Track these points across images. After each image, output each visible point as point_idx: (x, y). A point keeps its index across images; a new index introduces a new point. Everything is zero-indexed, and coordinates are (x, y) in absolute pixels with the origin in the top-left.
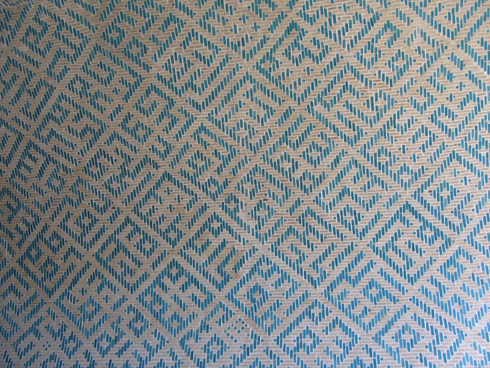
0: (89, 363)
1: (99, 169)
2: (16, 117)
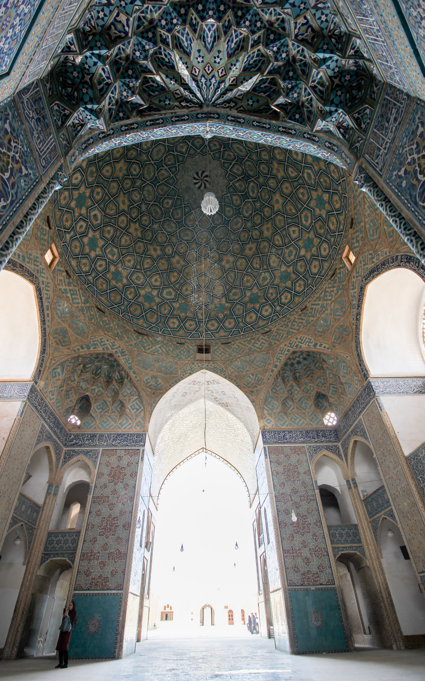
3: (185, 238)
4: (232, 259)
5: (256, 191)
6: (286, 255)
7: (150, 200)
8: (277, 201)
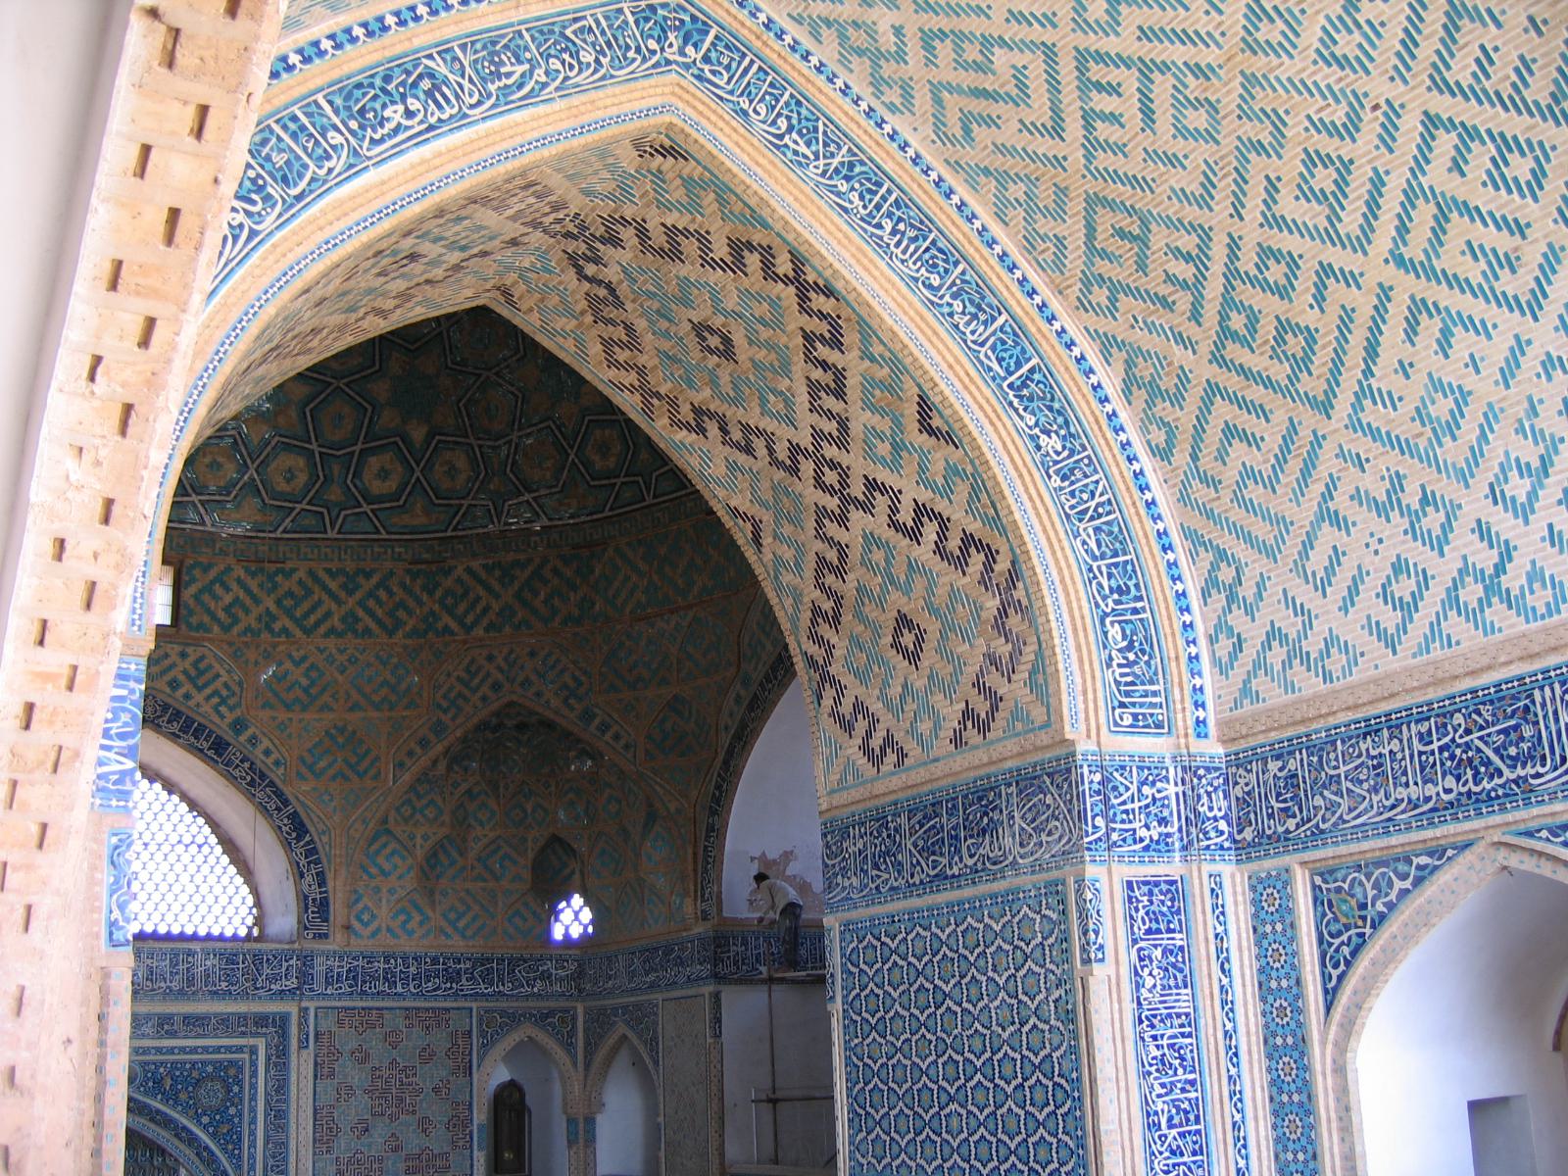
0: (1495, 552)
1: (1280, 25)
2: (1010, 11)
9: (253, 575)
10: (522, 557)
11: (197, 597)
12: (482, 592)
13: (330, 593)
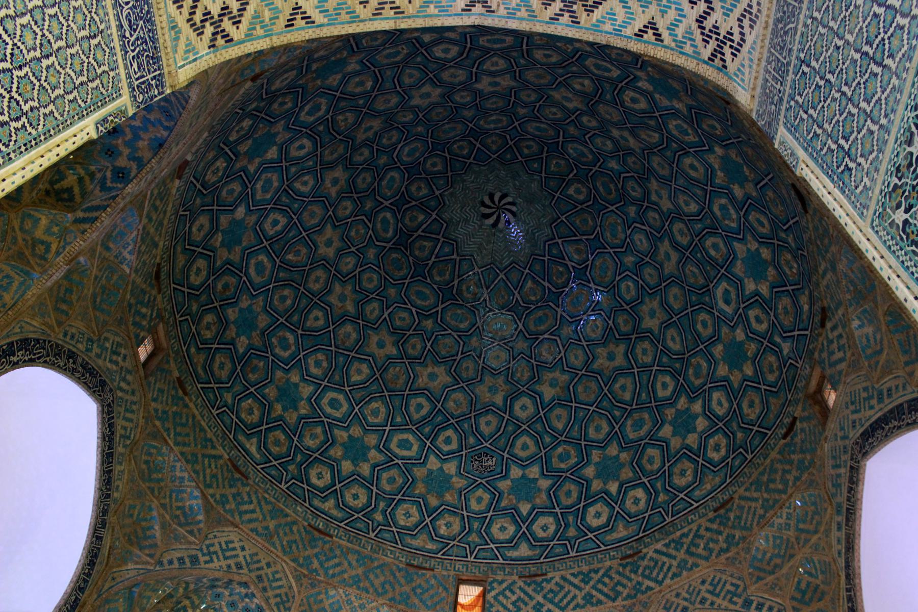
3: (542, 126)
4: (416, 101)
5: (379, 225)
6: (274, 178)
7: (615, 217)
8: (329, 243)
9: (529, 585)
10: (686, 530)
11: (495, 598)
12: (665, 559)
13: (575, 586)
